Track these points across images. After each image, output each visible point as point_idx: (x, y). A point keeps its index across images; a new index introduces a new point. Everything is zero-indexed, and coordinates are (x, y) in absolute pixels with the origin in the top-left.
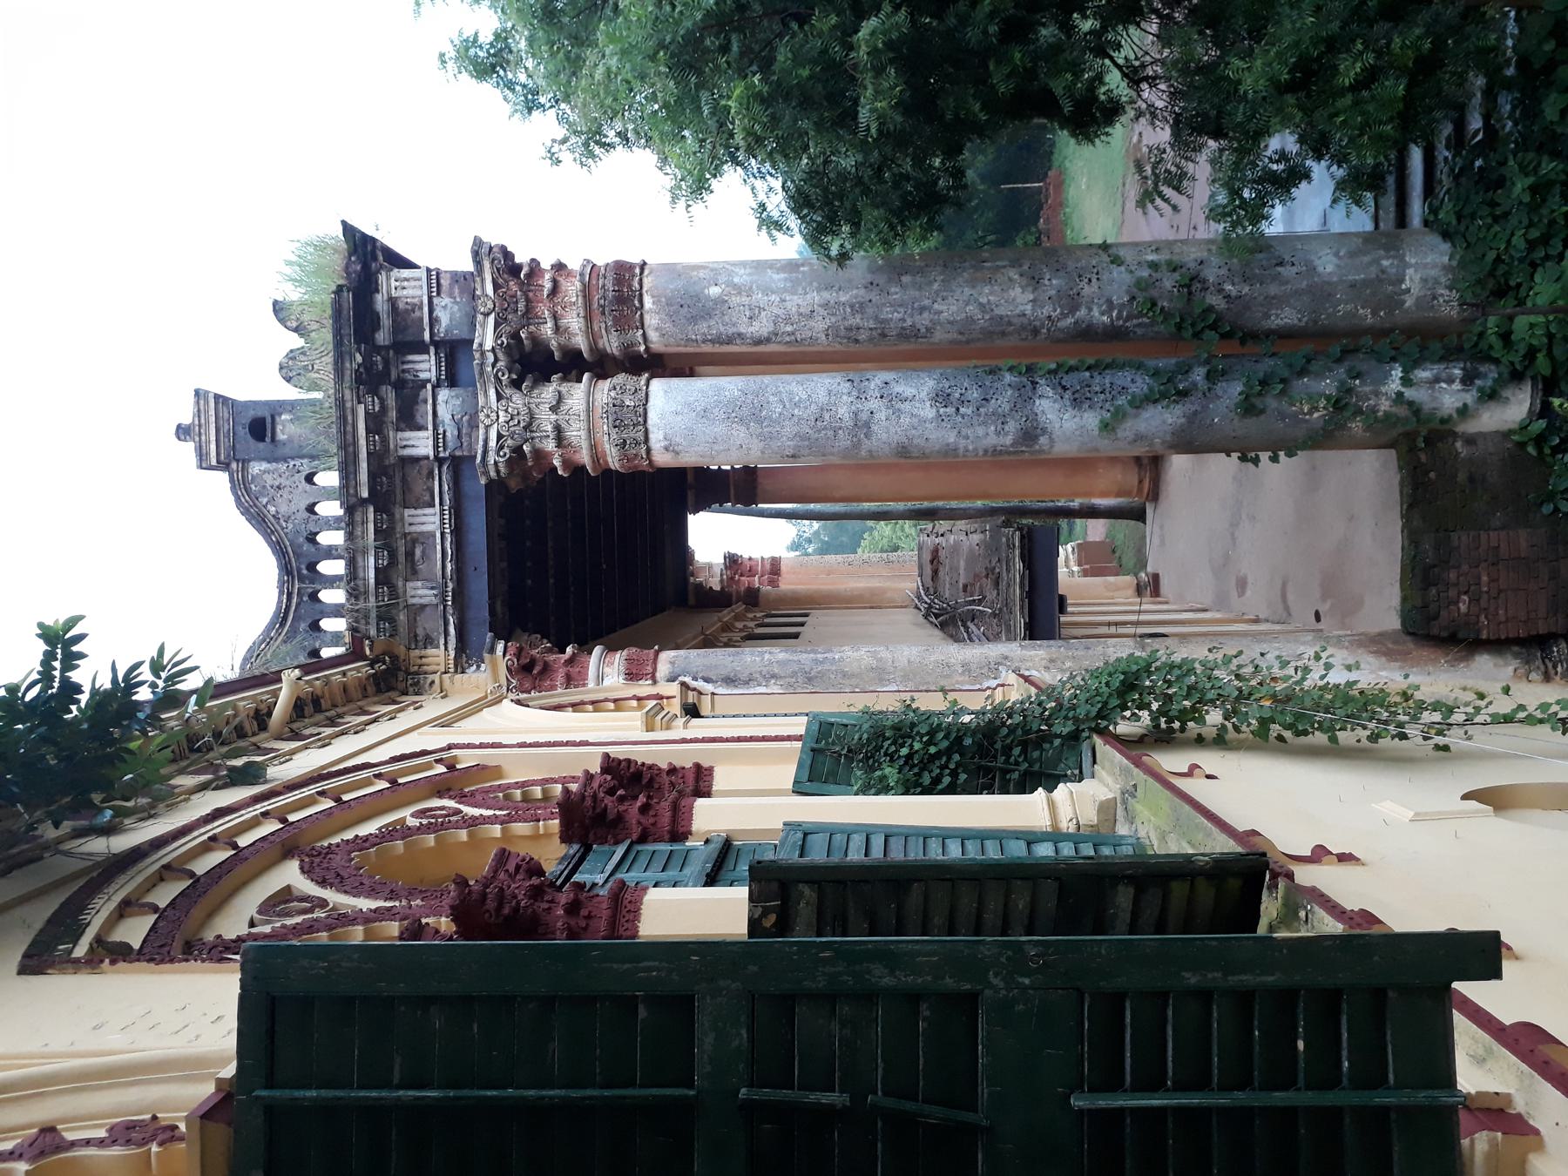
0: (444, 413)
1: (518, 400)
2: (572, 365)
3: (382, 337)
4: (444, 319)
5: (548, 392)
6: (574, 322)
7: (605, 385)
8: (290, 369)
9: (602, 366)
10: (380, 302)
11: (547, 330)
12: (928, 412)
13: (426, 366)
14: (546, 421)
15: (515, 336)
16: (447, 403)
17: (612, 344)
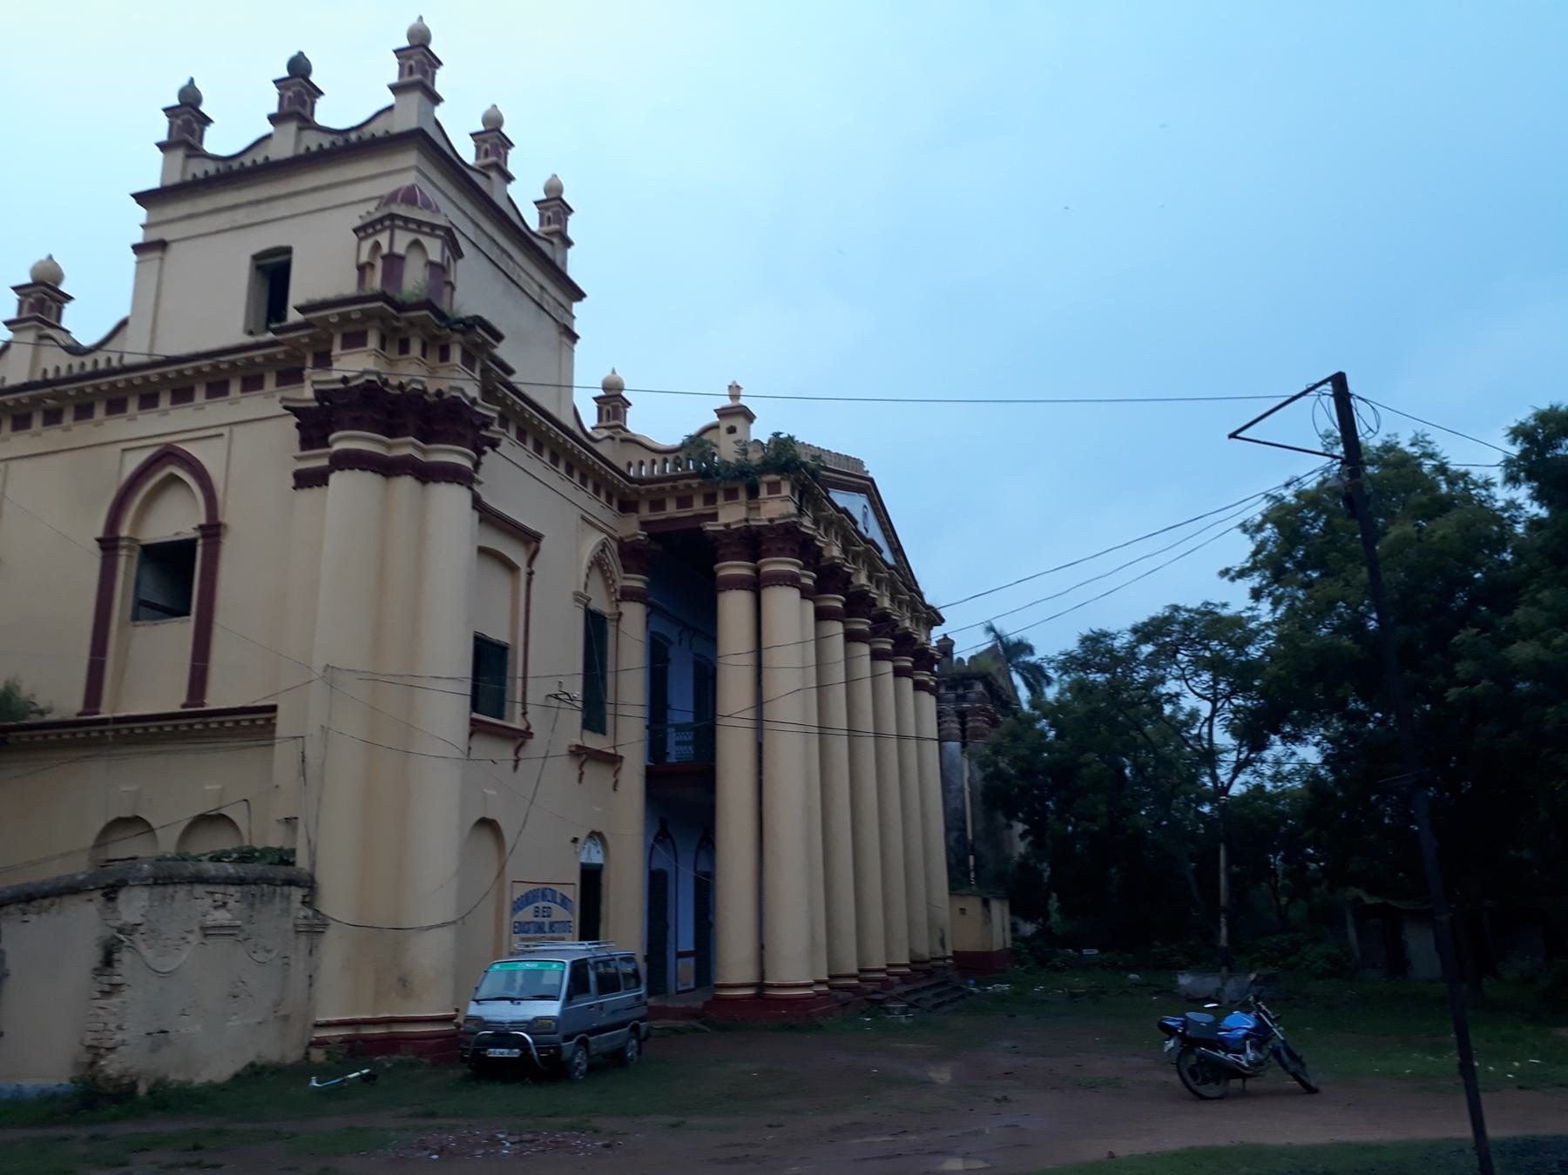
0: (949, 695)
1: (952, 712)
2: (963, 723)
3: (966, 682)
4: (970, 695)
5: (955, 719)
6: (970, 724)
7: (958, 732)
8: (960, 660)
9: (963, 731)
10: (973, 681)
11: (969, 718)
12: (953, 806)
13: (960, 691)
14: (948, 719)
15: (967, 711)
16: (951, 696)
17: (967, 733)
